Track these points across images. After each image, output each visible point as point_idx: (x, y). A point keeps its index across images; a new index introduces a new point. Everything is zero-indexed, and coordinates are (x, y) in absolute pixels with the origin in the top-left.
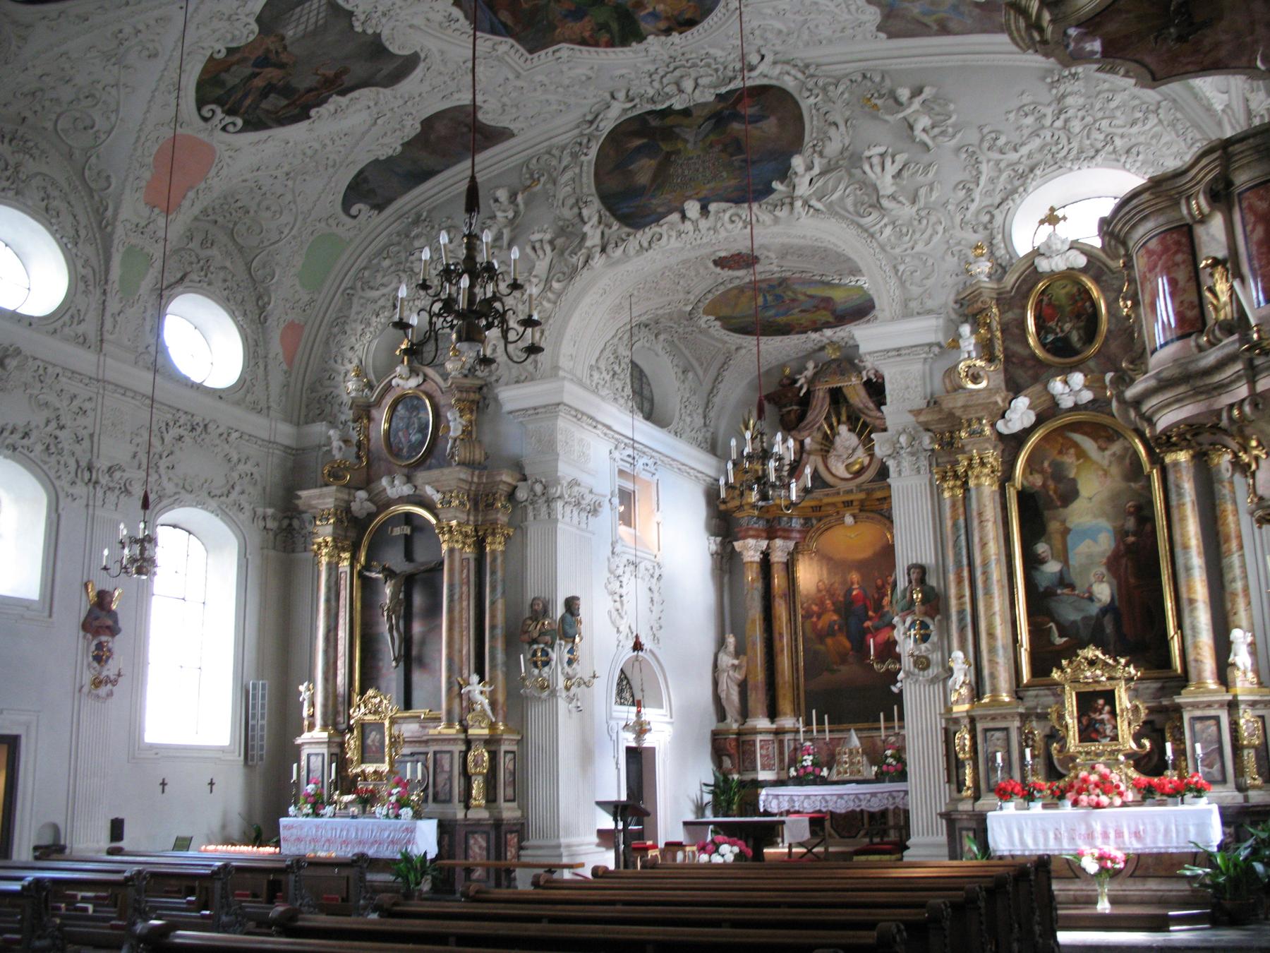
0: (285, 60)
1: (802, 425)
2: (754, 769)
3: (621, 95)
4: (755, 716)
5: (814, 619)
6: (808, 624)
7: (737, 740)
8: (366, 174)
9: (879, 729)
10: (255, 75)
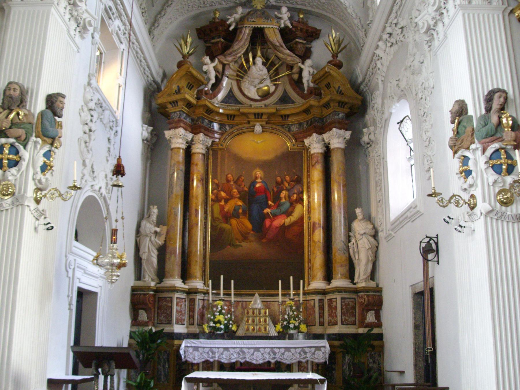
1: (228, 52)
2: (170, 323)
4: (172, 276)
5: (222, 203)
6: (217, 207)
7: (154, 296)
9: (278, 295)
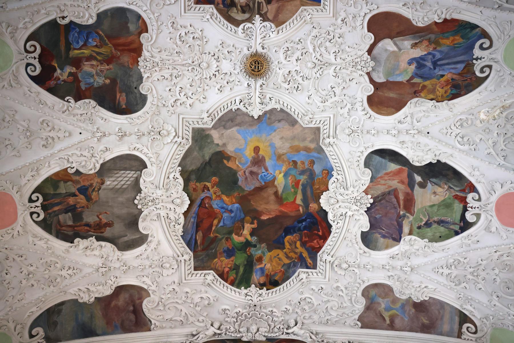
0: (93, 197)
3: (216, 325)
8: (64, 307)
10: (74, 195)
